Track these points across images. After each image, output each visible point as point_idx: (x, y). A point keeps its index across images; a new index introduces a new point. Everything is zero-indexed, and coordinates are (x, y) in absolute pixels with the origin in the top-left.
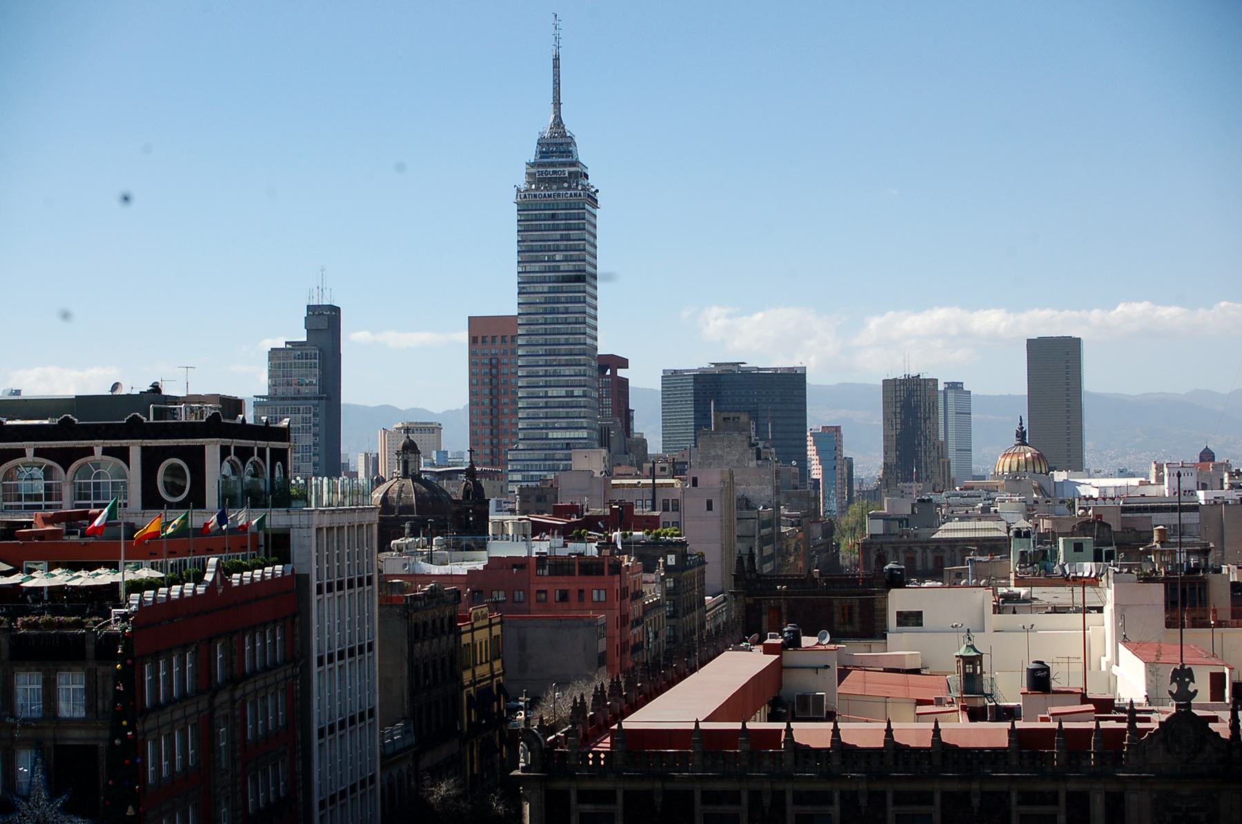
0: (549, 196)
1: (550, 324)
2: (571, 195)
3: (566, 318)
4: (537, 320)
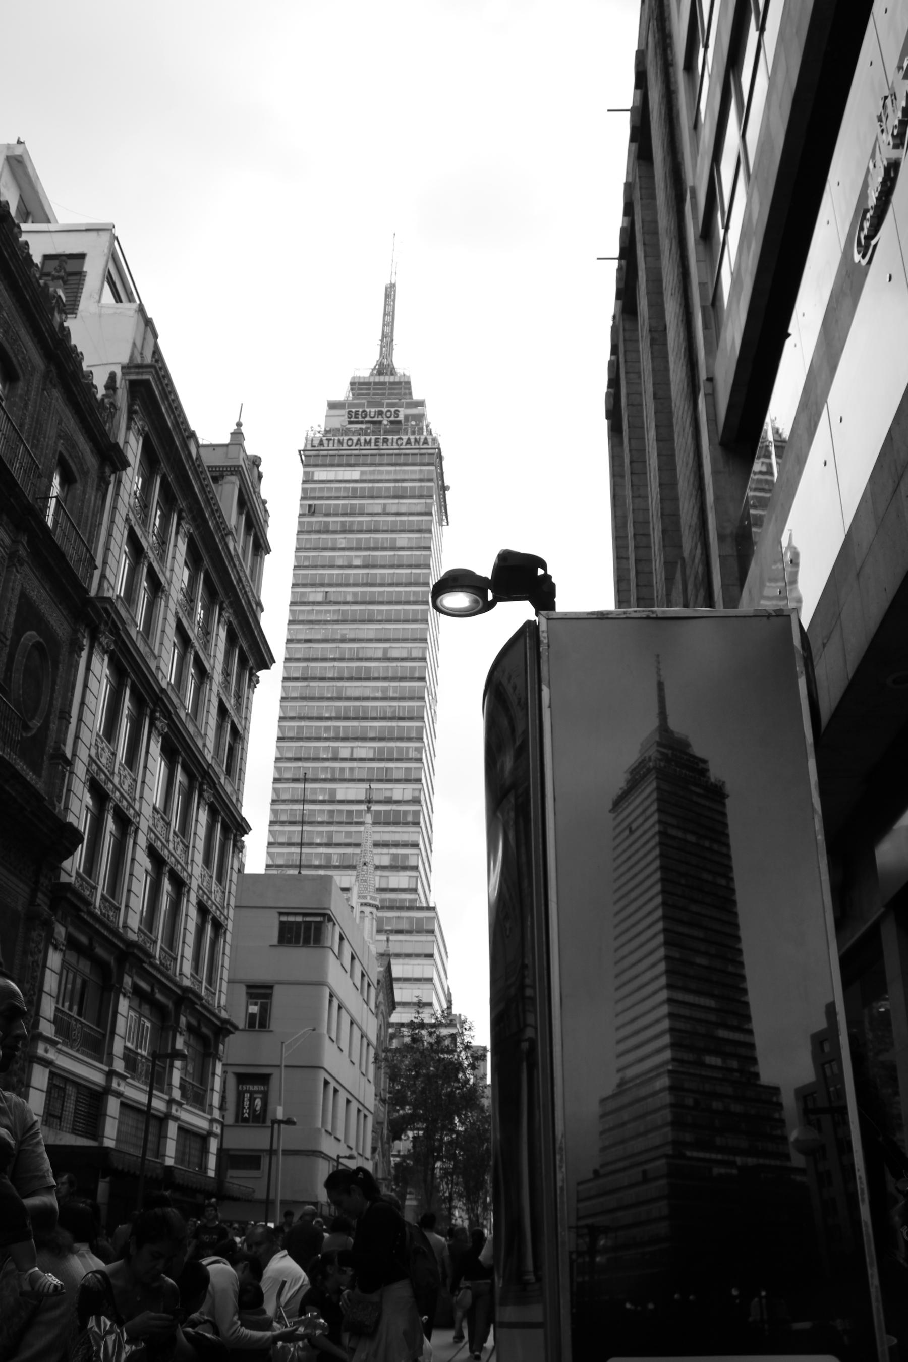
0: (368, 443)
2: (408, 442)
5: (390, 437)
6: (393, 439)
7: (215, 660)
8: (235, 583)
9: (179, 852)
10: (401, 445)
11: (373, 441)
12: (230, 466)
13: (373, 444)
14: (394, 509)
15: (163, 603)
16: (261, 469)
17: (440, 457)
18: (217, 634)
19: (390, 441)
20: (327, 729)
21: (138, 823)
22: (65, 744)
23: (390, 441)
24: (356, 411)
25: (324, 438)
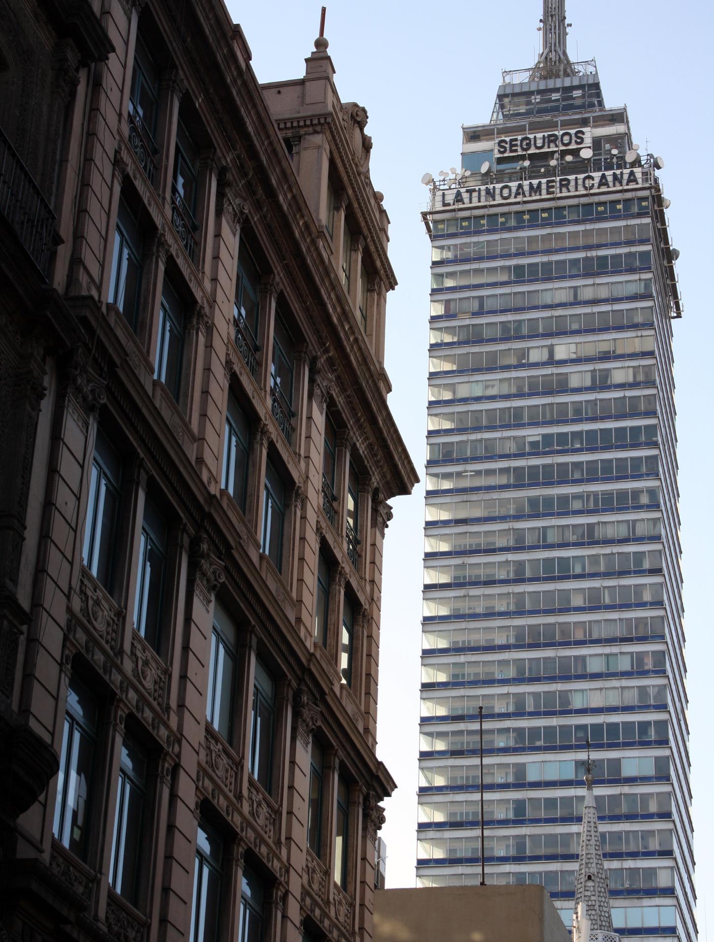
2: (603, 182)
3: (591, 526)
5: (572, 177)
6: (576, 179)
7: (307, 465)
8: (335, 320)
9: (261, 821)
10: (592, 187)
11: (544, 186)
12: (311, 118)
13: (544, 192)
14: (587, 294)
15: (202, 339)
16: (367, 131)
17: (658, 200)
18: (310, 418)
19: (573, 183)
20: (503, 663)
21: (179, 756)
22: (15, 582)
23: (573, 183)
24: (511, 140)
25: (463, 190)
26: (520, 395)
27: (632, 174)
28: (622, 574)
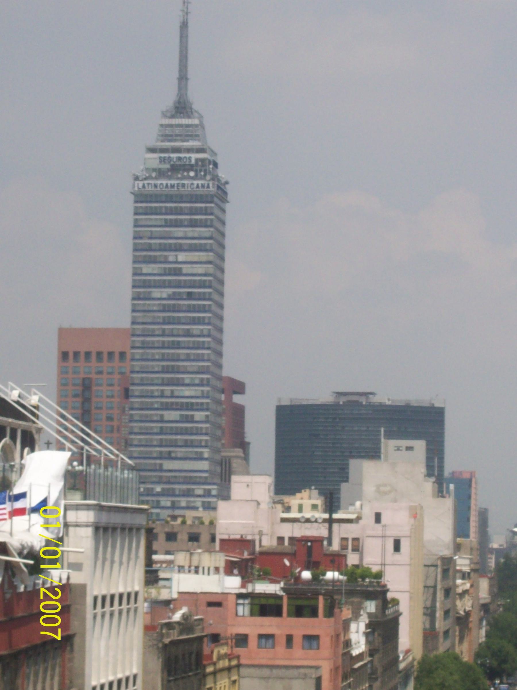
0: (172, 186)
1: (169, 336)
2: (198, 187)
4: (153, 330)
11: (176, 185)
13: (176, 188)
14: (190, 235)
19: (186, 185)
24: (165, 157)
26: (165, 274)
27: (208, 184)
28: (198, 348)
